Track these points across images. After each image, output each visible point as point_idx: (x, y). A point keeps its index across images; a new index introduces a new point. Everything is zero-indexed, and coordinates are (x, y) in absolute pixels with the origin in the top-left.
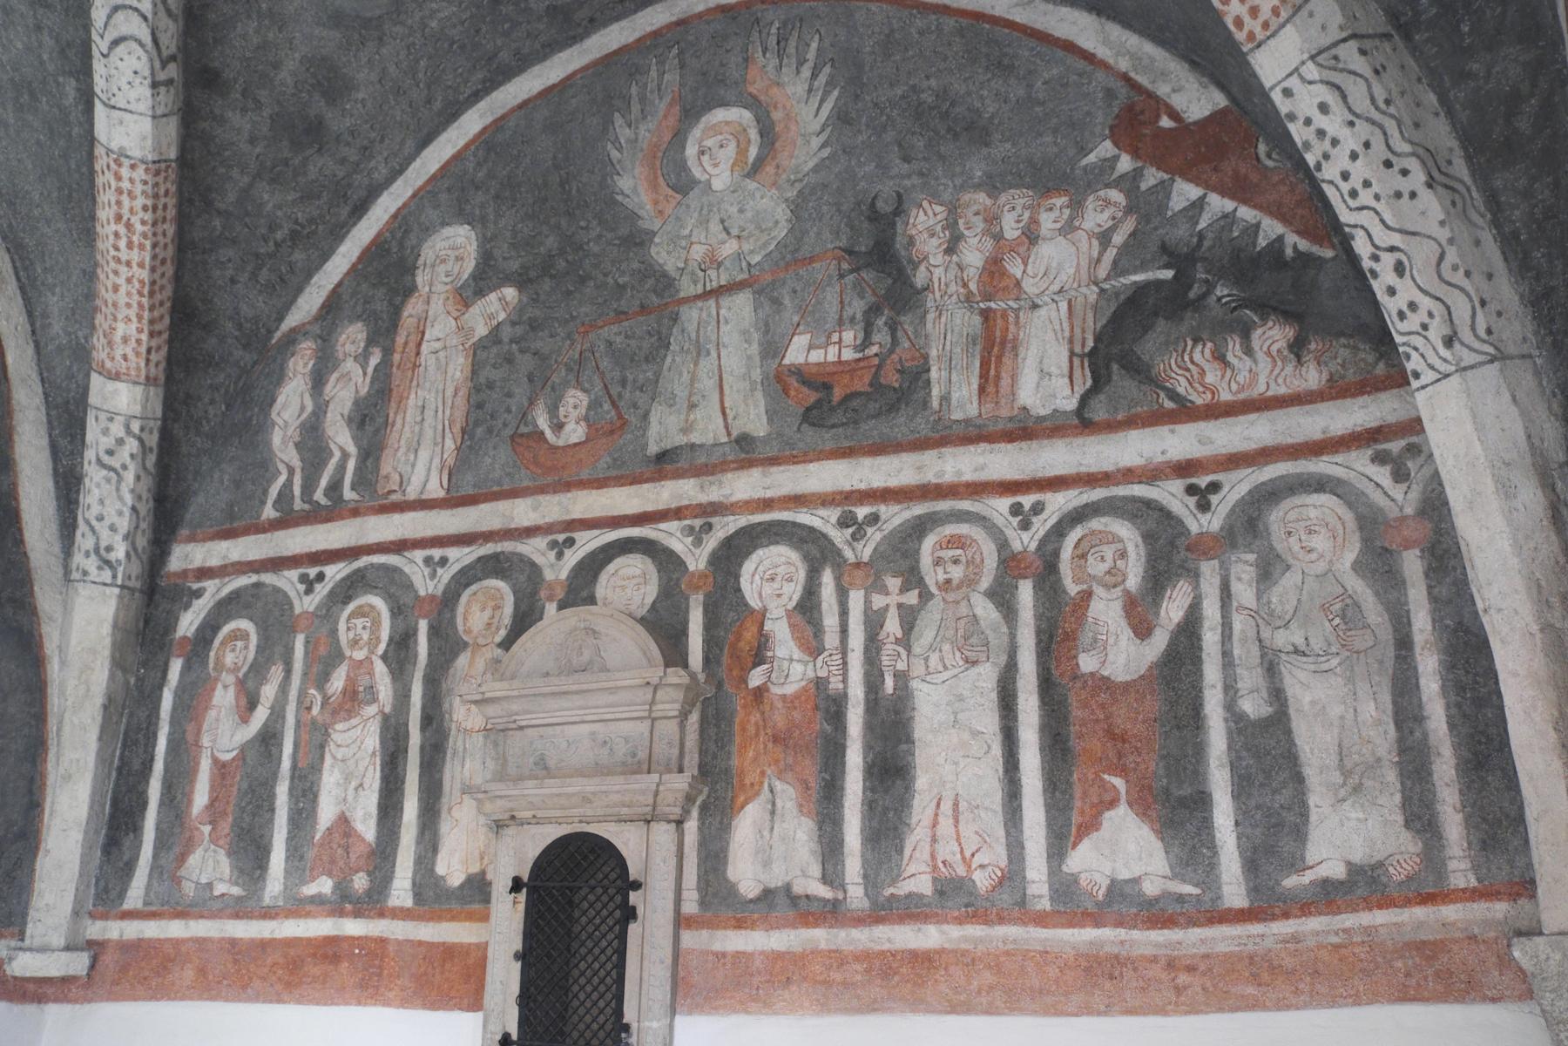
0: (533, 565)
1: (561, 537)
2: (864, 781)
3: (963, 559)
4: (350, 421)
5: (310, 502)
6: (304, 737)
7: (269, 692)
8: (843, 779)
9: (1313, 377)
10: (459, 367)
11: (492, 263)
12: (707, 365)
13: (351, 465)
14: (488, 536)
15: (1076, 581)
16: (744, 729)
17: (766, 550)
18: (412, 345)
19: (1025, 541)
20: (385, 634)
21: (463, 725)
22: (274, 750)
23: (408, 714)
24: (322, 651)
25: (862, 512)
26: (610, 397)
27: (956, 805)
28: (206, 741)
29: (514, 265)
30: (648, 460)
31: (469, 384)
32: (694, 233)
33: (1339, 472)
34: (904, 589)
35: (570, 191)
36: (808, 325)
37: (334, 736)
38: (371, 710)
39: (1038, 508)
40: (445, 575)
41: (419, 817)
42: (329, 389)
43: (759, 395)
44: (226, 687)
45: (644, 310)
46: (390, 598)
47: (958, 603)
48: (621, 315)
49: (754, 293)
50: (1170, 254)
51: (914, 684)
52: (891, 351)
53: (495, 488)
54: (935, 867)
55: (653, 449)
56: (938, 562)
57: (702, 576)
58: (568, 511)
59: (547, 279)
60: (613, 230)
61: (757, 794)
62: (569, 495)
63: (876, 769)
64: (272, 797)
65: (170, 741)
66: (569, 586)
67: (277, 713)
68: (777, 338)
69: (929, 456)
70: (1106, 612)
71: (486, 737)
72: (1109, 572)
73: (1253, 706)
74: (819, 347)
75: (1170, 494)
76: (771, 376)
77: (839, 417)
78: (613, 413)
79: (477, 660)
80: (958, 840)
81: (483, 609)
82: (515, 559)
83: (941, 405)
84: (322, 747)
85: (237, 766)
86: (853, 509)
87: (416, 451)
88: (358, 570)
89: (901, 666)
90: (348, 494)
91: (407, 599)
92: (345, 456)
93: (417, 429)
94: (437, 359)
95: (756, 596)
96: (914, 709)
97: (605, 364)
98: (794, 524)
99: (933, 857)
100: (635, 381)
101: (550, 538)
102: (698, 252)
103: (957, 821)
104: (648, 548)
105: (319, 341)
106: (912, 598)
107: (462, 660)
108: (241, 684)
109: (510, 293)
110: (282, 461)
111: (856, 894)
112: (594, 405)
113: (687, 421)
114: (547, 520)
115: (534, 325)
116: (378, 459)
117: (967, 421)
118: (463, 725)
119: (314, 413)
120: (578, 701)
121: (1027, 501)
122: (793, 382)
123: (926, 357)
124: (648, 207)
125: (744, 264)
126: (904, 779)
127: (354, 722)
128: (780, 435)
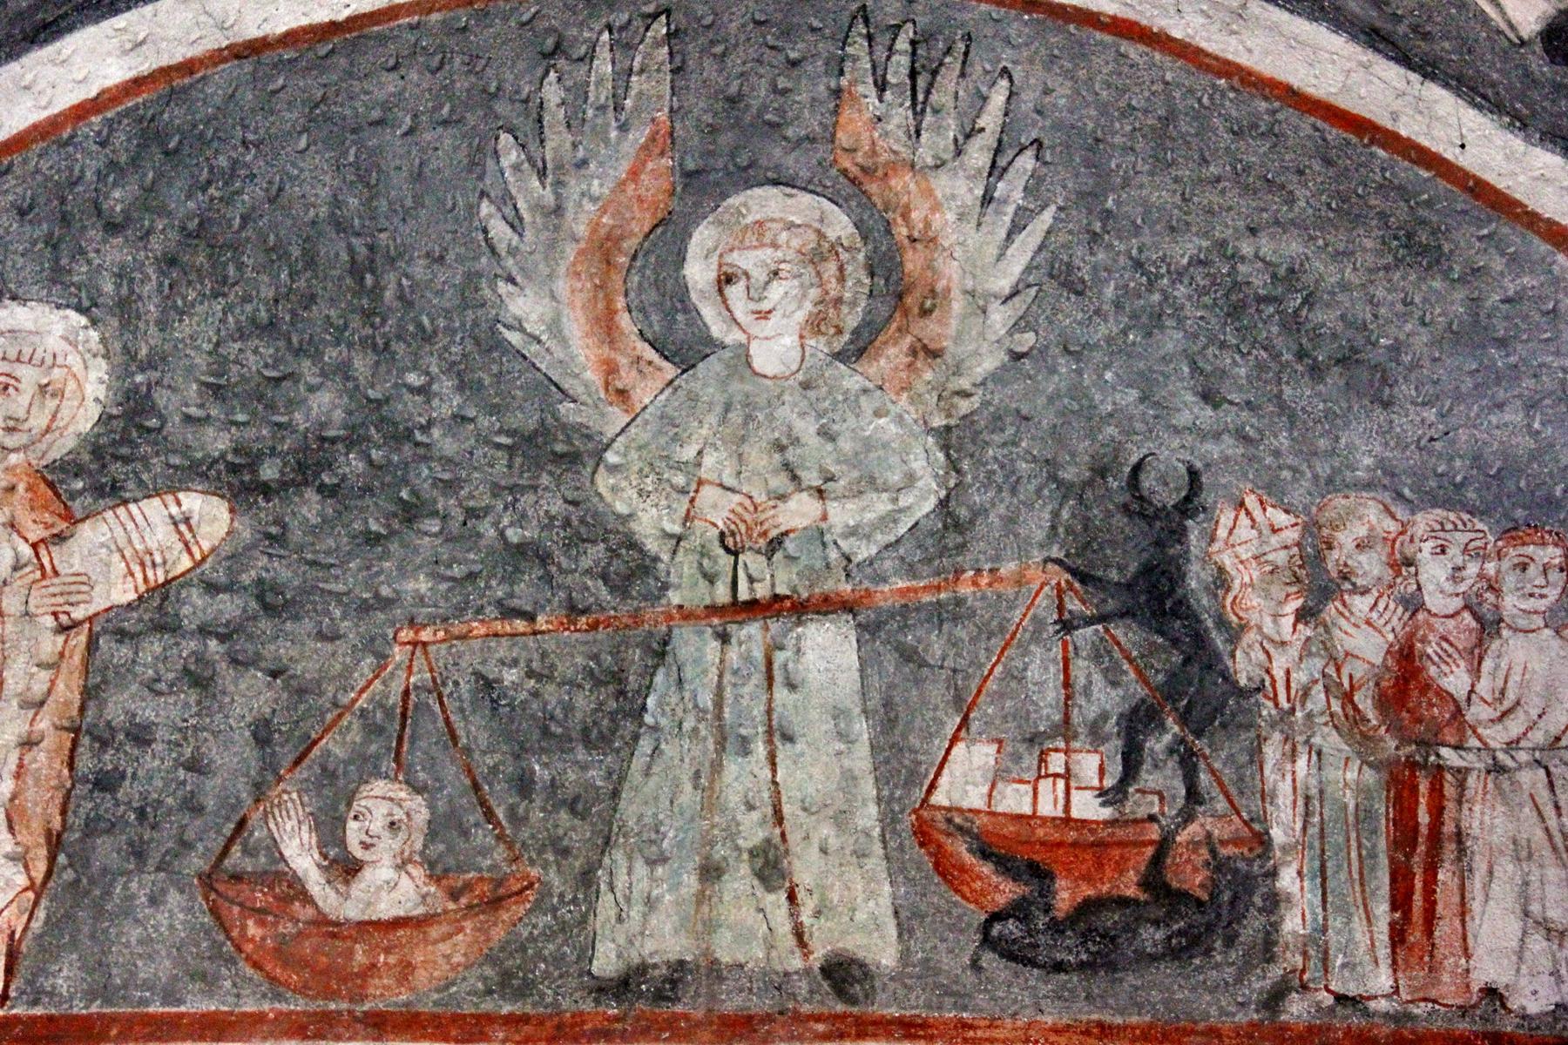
11: (153, 422)
32: (709, 460)
35: (378, 289)
49: (859, 625)
55: (606, 962)
59: (311, 494)
60: (494, 410)
68: (914, 741)
97: (475, 729)
122: (961, 849)
124: (589, 375)
125: (833, 555)
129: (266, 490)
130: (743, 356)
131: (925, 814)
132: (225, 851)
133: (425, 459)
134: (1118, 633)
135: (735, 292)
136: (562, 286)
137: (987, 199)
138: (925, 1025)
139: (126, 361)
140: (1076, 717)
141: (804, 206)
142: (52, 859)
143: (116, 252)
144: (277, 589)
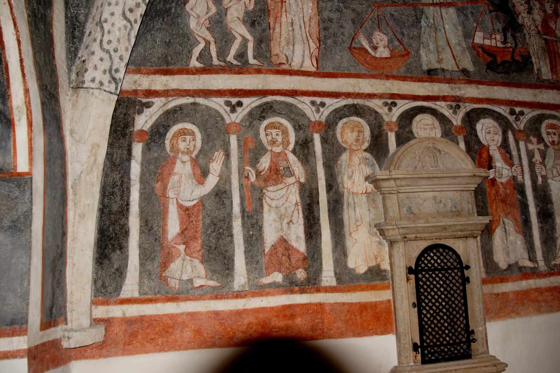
0: (376, 112)
1: (389, 101)
2: (538, 219)
3: (557, 133)
4: (244, 22)
5: (225, 61)
6: (247, 194)
7: (216, 167)
8: (530, 218)
13: (251, 46)
14: (348, 95)
16: (490, 197)
17: (484, 120)
21: (351, 190)
22: (227, 202)
23: (317, 183)
24: (251, 145)
25: (517, 109)
26: (398, 39)
28: (171, 194)
34: (539, 143)
36: (480, 28)
38: (292, 180)
40: (326, 112)
41: (332, 238)
43: (468, 53)
44: (184, 162)
46: (290, 120)
51: (550, 181)
53: (346, 72)
55: (425, 68)
56: (548, 133)
57: (461, 128)
58: (390, 90)
61: (499, 224)
62: (389, 81)
63: (541, 215)
64: (230, 228)
65: (141, 194)
66: (399, 124)
67: (225, 179)
71: (368, 197)
74: (487, 39)
76: (471, 45)
78: (401, 47)
79: (353, 157)
81: (352, 131)
82: (365, 108)
83: (538, 73)
84: (261, 200)
85: (199, 211)
86: (514, 108)
87: (294, 45)
88: (266, 103)
89: (544, 173)
90: (252, 61)
91: (305, 122)
92: (245, 41)
93: (291, 33)
95: (484, 139)
96: (551, 191)
97: (391, 23)
98: (494, 111)
101: (383, 101)
104: (434, 112)
106: (541, 147)
107: (345, 157)
108: (195, 162)
110: (199, 36)
111: (541, 264)
112: (390, 41)
113: (439, 58)
114: (379, 92)
116: (269, 46)
117: (548, 80)
118: (351, 190)
120: (436, 181)
122: (480, 50)
123: (529, 52)
126: (551, 218)
127: (280, 186)
131: (474, 44)
134: (499, 14)
138: (481, 82)
140: (495, 29)
142: (320, 43)
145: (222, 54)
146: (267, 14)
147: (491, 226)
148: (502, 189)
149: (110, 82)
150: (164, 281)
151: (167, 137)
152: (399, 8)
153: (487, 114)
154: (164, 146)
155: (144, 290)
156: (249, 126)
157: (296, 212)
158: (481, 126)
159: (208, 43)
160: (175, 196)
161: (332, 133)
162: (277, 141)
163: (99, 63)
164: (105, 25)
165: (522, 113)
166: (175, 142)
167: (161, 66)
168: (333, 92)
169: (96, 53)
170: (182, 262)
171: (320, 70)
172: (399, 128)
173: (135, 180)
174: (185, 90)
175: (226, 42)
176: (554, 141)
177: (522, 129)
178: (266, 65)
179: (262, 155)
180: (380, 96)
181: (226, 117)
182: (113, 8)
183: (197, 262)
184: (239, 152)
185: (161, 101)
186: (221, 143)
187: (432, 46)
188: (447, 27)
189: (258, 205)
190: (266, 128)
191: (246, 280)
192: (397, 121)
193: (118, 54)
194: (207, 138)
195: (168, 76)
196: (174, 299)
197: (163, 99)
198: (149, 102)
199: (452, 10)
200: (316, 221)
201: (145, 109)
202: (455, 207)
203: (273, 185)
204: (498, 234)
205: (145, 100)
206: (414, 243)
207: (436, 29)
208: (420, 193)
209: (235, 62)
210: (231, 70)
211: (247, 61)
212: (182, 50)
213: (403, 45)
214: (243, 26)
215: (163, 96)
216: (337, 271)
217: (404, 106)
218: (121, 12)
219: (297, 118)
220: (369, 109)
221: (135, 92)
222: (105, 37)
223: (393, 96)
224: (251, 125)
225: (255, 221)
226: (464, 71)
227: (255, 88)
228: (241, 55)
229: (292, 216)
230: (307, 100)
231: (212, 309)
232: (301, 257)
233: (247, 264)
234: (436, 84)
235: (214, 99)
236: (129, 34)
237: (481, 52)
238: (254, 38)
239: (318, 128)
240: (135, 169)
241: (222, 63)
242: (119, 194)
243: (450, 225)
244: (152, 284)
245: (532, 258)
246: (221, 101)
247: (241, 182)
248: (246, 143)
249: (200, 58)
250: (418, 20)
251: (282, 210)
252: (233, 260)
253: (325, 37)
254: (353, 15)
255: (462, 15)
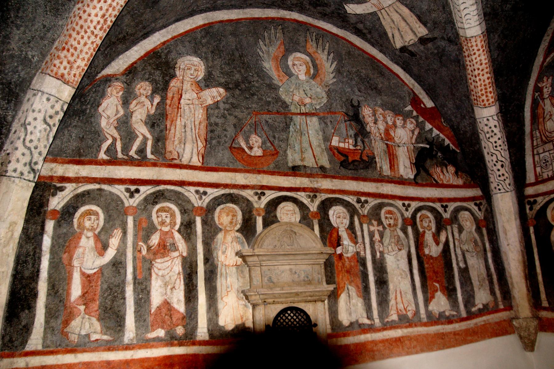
0: (248, 200)
1: (259, 191)
4: (146, 123)
5: (127, 155)
6: (139, 265)
7: (114, 242)
8: (369, 285)
9: (460, 182)
10: (200, 114)
11: (213, 76)
12: (305, 138)
13: (150, 143)
14: (226, 186)
15: (422, 228)
16: (337, 268)
18: (176, 99)
19: (408, 214)
20: (178, 220)
21: (224, 263)
22: (122, 271)
23: (197, 257)
24: (144, 225)
25: (363, 199)
26: (270, 141)
27: (401, 293)
28: (76, 263)
29: (223, 80)
30: (289, 168)
31: (206, 122)
32: (295, 91)
33: (469, 207)
34: (378, 225)
36: (337, 134)
37: (156, 265)
38: (176, 254)
39: (409, 205)
40: (207, 200)
41: (207, 301)
42: (132, 106)
43: (325, 153)
44: (88, 238)
45: (278, 113)
46: (178, 205)
47: (394, 231)
48: (269, 112)
50: (427, 141)
51: (386, 255)
52: (364, 149)
53: (226, 167)
54: (398, 312)
55: (290, 165)
56: (386, 218)
57: (316, 213)
58: (261, 182)
59: (237, 90)
60: (263, 80)
61: (344, 290)
62: (260, 175)
64: (123, 292)
65: (51, 263)
66: (266, 210)
67: (121, 251)
69: (379, 184)
70: (429, 237)
71: (237, 269)
72: (428, 226)
73: (462, 265)
74: (342, 142)
75: (438, 206)
76: (328, 147)
77: (351, 167)
78: (272, 147)
79: (227, 236)
80: (403, 303)
81: (228, 215)
82: (240, 197)
84: (150, 269)
85: (98, 277)
87: (185, 144)
88: (160, 191)
89: (381, 249)
90: (149, 156)
91: (189, 207)
92: (145, 139)
93: (183, 134)
94: (189, 108)
97: (266, 128)
98: (344, 200)
99: (397, 309)
100: (279, 138)
101: (254, 191)
102: (296, 98)
103: (402, 297)
104: (295, 201)
105: (125, 85)
106: (381, 228)
107: (220, 236)
108: (97, 237)
109: (222, 90)
111: (377, 321)
112: (264, 143)
114: (251, 183)
115: (234, 106)
116: (164, 144)
117: (388, 176)
118: (224, 263)
119: (125, 115)
120: (292, 257)
121: (406, 203)
122: (336, 151)
123: (374, 154)
127: (166, 259)
128: (334, 169)
129: (230, 88)
130: (297, 76)
132: (232, 144)
133: (254, 86)
135: (295, 67)
136: (271, 63)
137: (328, 59)
139: (207, 67)
141: (303, 56)
143: (204, 50)
144: (234, 104)
145: (126, 149)
146: (165, 118)
147: (338, 292)
148: (347, 263)
149: (29, 172)
150: (65, 336)
151: (75, 216)
152: (273, 116)
153: (338, 202)
154: (72, 224)
155: (47, 343)
156: (144, 209)
157: (178, 280)
158: (333, 212)
159: (115, 140)
160: (79, 265)
161: (211, 216)
162: (166, 222)
163: (21, 157)
164: (28, 127)
165: (366, 202)
166: (82, 221)
167: (74, 157)
168: (214, 184)
169: (19, 149)
170: (81, 320)
171: (205, 165)
172: (266, 213)
173: (46, 251)
174: (93, 178)
175: (130, 139)
176: (390, 224)
177: (366, 214)
178: (161, 159)
179: (152, 233)
180: (252, 187)
181: (125, 201)
182: (35, 115)
183: (94, 320)
184: (134, 230)
185: (72, 186)
186: (120, 223)
187: (297, 147)
188: (310, 132)
189: (147, 274)
190: (157, 212)
191: (135, 335)
192: (264, 208)
193: (38, 150)
194: (109, 218)
195: (79, 166)
196: (73, 351)
197: (74, 185)
198: (62, 187)
199: (315, 119)
200: (194, 287)
201: (58, 193)
202: (307, 277)
203: (161, 258)
204: (343, 299)
205: (59, 185)
206: (273, 306)
207: (301, 133)
208: (279, 266)
209: (136, 157)
210: (132, 163)
211: (146, 156)
212: (93, 145)
213: (274, 146)
214: (145, 127)
215: (74, 182)
216: (210, 329)
217: (271, 195)
218: (42, 118)
219: (184, 204)
220: (243, 197)
221: (51, 178)
222: (28, 136)
223: (263, 187)
224: (145, 209)
225: (144, 287)
226: (322, 168)
227: (151, 179)
228: (141, 151)
229: (175, 283)
230: (192, 189)
231: (104, 359)
232: (181, 317)
233: (136, 322)
234: (298, 178)
235: (117, 186)
236: (48, 135)
237: (336, 153)
238: (153, 137)
239: (200, 212)
240: (47, 242)
241: (125, 157)
242: (31, 262)
243: (301, 292)
244: (54, 338)
245: (370, 317)
246: (122, 188)
247: (135, 255)
248: (140, 223)
249: (107, 151)
250: (287, 126)
251: (167, 278)
252: (124, 319)
253: (211, 138)
254: (235, 121)
255: (323, 124)
